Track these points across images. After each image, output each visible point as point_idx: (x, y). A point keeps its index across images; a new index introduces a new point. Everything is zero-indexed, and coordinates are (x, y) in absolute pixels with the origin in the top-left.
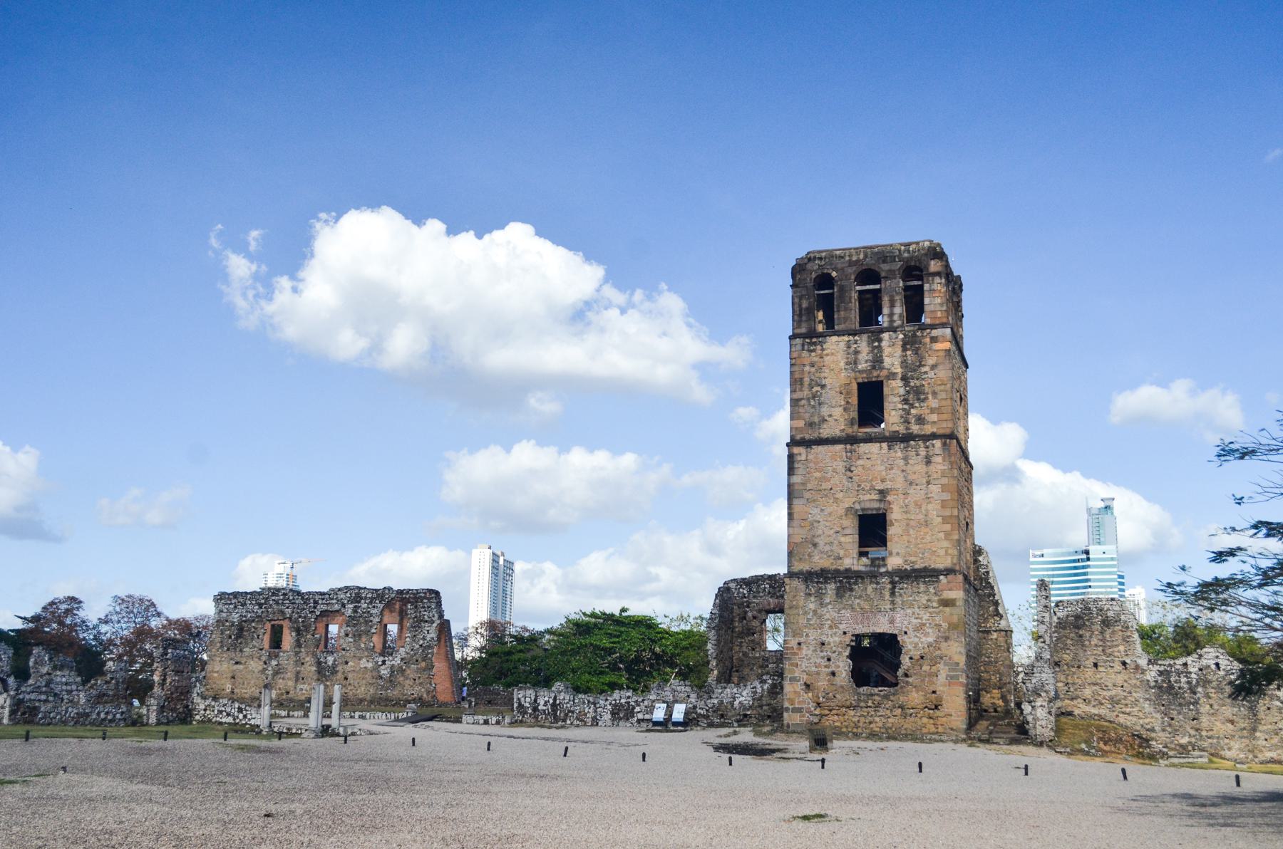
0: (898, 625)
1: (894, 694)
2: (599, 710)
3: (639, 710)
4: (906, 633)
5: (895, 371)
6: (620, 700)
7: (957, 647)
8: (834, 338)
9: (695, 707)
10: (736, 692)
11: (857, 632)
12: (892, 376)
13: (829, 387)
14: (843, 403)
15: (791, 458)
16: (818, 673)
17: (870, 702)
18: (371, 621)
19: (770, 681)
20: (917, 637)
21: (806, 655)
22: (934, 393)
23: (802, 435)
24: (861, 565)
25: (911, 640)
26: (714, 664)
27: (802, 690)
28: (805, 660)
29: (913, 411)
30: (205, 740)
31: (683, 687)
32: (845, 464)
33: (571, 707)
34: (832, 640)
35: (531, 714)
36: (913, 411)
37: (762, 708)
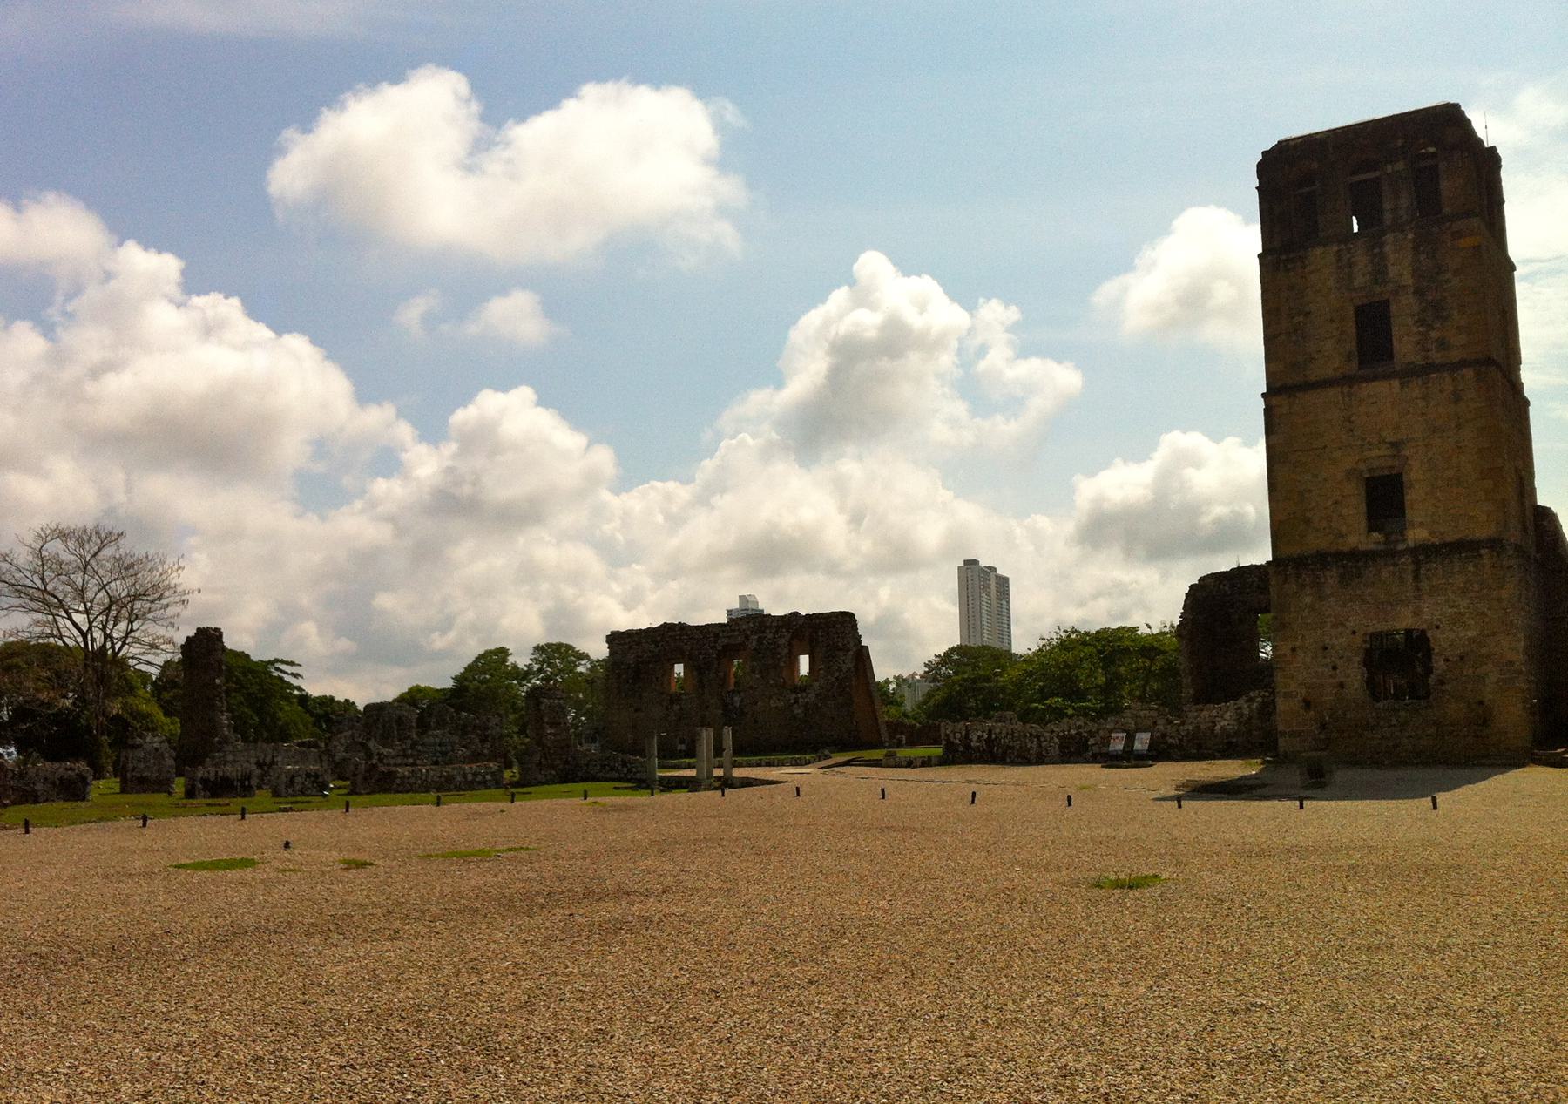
2: (1045, 743)
5: (1404, 283)
6: (1069, 731)
8: (1319, 251)
9: (1164, 735)
11: (1371, 630)
15: (1269, 413)
17: (1393, 719)
18: (779, 654)
19: (1259, 699)
20: (1454, 632)
24: (1374, 541)
26: (1189, 681)
27: (1301, 708)
30: (622, 797)
31: (1147, 712)
34: (1336, 642)
36: (1434, 334)
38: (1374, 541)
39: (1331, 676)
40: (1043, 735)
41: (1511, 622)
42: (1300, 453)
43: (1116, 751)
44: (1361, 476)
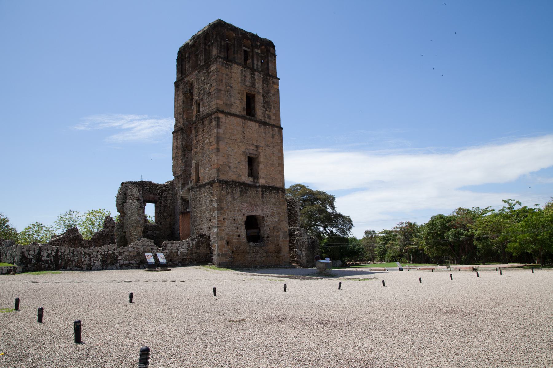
0: (265, 212)
1: (264, 246)
2: (93, 259)
3: (121, 258)
4: (268, 216)
5: (260, 91)
6: (108, 252)
7: (286, 224)
8: (236, 66)
10: (179, 246)
12: (258, 92)
13: (234, 89)
14: (240, 99)
16: (233, 235)
17: (254, 250)
19: (196, 240)
21: (228, 225)
22: (274, 107)
23: (222, 109)
24: (248, 180)
25: (270, 220)
28: (227, 228)
29: (267, 112)
31: (149, 243)
32: (242, 129)
33: (71, 257)
34: (238, 218)
35: (34, 264)
36: (267, 112)
37: (192, 255)
38: (248, 180)
39: (237, 232)
40: (92, 254)
41: (286, 217)
42: (228, 139)
43: (152, 262)
44: (247, 155)
